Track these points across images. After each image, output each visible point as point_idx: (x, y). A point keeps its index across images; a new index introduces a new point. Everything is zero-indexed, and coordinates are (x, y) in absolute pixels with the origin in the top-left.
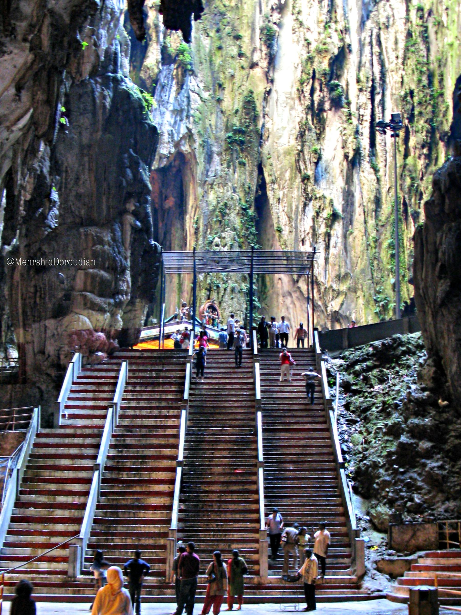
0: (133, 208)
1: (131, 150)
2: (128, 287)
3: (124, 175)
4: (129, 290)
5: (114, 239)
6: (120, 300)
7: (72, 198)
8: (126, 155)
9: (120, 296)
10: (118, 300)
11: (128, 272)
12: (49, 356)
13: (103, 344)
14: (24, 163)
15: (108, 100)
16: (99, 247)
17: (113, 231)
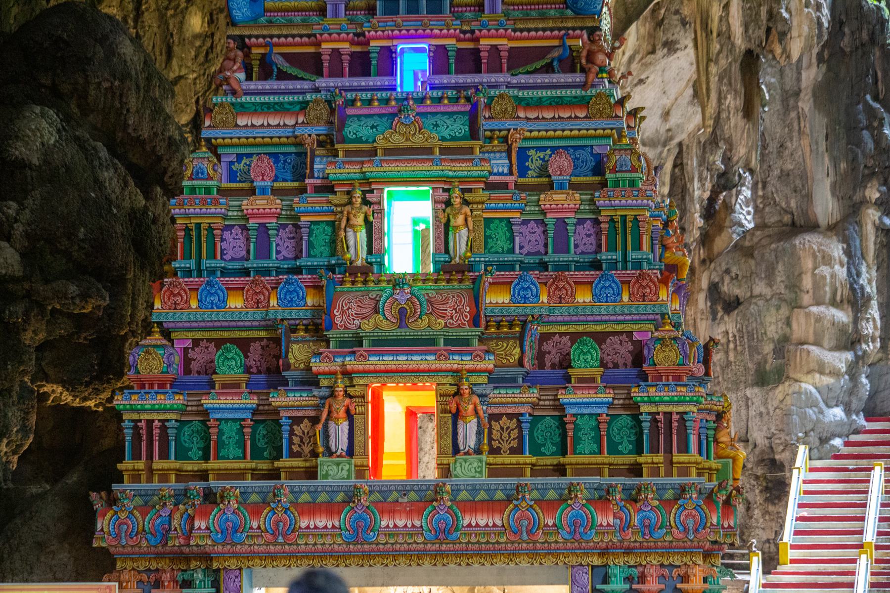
0: (877, 195)
1: (868, 97)
2: (875, 327)
3: (859, 143)
4: (878, 333)
5: (848, 253)
6: (865, 352)
7: (773, 180)
8: (861, 107)
9: (864, 346)
10: (860, 353)
11: (874, 303)
12: (755, 446)
13: (841, 423)
14: (702, 161)
15: (826, 11)
16: (825, 270)
17: (846, 240)
